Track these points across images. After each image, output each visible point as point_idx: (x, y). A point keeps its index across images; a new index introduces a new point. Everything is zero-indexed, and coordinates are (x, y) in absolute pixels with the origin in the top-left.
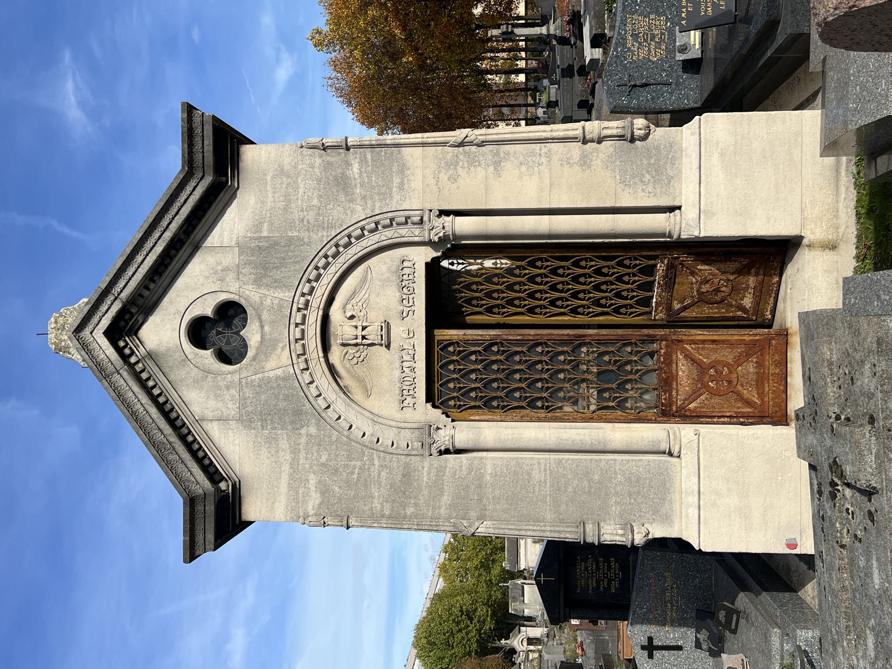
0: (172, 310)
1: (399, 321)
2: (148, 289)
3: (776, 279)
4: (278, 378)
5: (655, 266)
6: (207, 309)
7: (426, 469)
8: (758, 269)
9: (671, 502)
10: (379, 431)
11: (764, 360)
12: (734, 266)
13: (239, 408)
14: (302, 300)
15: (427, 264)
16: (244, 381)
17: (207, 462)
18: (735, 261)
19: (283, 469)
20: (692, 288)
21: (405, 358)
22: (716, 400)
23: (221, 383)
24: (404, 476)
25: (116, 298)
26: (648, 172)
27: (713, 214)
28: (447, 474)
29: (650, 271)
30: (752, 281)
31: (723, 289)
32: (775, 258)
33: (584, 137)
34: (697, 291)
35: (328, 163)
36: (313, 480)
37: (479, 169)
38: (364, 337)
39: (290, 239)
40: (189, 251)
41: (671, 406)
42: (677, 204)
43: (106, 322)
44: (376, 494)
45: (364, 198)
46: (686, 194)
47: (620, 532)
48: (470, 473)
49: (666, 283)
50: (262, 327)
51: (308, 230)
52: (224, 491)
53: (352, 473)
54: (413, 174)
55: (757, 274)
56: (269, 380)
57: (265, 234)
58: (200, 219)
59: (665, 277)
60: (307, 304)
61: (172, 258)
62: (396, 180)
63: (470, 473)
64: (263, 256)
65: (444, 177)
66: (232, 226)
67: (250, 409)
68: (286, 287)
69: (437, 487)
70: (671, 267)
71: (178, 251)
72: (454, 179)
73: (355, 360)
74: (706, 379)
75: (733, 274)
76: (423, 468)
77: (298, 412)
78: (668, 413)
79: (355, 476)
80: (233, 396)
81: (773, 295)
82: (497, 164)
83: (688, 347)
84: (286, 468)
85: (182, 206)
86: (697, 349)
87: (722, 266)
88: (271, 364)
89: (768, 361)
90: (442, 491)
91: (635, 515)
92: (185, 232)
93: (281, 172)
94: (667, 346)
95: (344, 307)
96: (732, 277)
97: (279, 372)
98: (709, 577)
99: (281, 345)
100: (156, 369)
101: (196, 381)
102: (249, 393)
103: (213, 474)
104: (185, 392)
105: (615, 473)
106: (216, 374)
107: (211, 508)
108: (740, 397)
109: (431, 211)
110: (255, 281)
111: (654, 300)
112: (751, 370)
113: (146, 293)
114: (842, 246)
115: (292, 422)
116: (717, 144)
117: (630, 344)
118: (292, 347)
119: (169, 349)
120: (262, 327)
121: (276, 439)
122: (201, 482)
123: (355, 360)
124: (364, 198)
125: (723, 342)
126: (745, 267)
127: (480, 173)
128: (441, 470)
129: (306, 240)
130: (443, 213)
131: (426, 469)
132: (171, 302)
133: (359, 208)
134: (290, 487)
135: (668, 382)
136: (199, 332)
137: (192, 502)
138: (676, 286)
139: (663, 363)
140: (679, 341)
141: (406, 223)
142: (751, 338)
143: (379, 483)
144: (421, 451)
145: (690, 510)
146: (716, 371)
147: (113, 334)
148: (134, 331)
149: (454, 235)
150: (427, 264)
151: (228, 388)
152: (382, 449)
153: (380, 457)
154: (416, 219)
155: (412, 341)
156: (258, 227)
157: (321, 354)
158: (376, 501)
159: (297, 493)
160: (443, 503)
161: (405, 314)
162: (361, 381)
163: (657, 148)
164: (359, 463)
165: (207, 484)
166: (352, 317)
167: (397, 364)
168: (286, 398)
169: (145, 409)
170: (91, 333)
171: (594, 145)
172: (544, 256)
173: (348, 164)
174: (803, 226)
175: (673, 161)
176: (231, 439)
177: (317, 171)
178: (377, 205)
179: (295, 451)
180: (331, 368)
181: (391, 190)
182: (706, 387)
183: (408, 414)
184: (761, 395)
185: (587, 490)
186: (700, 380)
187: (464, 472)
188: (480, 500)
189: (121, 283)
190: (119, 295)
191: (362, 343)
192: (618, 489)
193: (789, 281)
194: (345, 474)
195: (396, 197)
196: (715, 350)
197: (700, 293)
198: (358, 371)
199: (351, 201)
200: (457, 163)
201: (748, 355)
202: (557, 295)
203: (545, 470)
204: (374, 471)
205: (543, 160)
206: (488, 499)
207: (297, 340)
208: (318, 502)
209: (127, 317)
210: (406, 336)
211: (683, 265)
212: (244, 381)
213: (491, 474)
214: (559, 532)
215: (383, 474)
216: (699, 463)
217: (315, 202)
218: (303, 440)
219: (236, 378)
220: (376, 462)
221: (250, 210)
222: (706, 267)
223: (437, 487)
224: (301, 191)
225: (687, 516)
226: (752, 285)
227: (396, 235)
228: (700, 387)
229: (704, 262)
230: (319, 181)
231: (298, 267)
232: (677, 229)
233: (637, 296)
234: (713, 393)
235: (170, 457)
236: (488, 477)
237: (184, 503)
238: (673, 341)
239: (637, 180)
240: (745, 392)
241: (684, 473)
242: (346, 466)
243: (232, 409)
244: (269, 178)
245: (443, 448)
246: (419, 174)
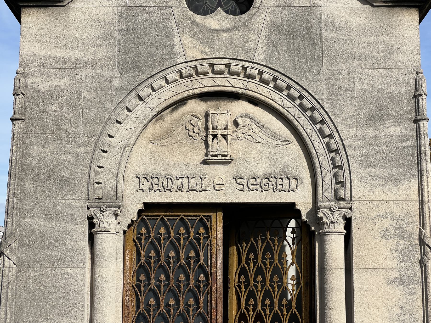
1: (232, 174)
4: (172, 46)
7: (74, 203)
19: (76, 51)
21: (192, 181)
24: (67, 179)
28: (68, 225)
35: (400, 101)
36: (63, 83)
37: (396, 261)
38: (215, 136)
39: (319, 60)
44: (47, 150)
48: (69, 250)
50: (226, 30)
51: (329, 79)
53: (71, 125)
54: (389, 190)
56: (170, 38)
57: (325, 34)
60: (251, 77)
62: (382, 172)
67: (140, 17)
68: (269, 56)
69: (55, 215)
72: (385, 234)
76: (75, 200)
77: (135, 67)
79: (67, 127)
82: (401, 281)
84: (77, 55)
90: (49, 219)
93: (390, 52)
95: (247, 116)
97: (178, 48)
99: (207, 50)
102: (156, 16)
109: (350, 209)
118: (205, 62)
120: (226, 30)
121: (107, 44)
124: (364, 138)
127: (392, 262)
128: (72, 219)
129: (318, 77)
131: (74, 203)
133: (353, 133)
134: (56, 59)
143: (59, 153)
144: (92, 197)
149: (325, 234)
150: (294, 204)
152: (95, 156)
154: (341, 194)
156: (333, 26)
157: (197, 91)
158: (40, 149)
159: (50, 67)
160: (36, 220)
161: (239, 180)
162: (168, 133)
164: (80, 131)
166: (236, 124)
167: (185, 172)
168: (151, 55)
173: (400, 121)
177: (392, 89)
178: (356, 152)
179: (94, 64)
180: (182, 102)
181: (373, 166)
183: (132, 184)
187: (70, 244)
188: (39, 261)
191: (209, 135)
194: (69, 117)
195: (365, 172)
199: (360, 125)
200: (401, 238)
204: (73, 148)
207: (212, 66)
208: (40, 87)
210: (216, 182)
212: (170, 11)
215: (69, 156)
217: (359, 87)
218: (106, 73)
220: (82, 150)
221: (349, 19)
224: (370, 72)
230: (381, 91)
231: (290, 68)
242: (78, 118)
244: (384, 38)
245: (95, 221)
246: (391, 196)
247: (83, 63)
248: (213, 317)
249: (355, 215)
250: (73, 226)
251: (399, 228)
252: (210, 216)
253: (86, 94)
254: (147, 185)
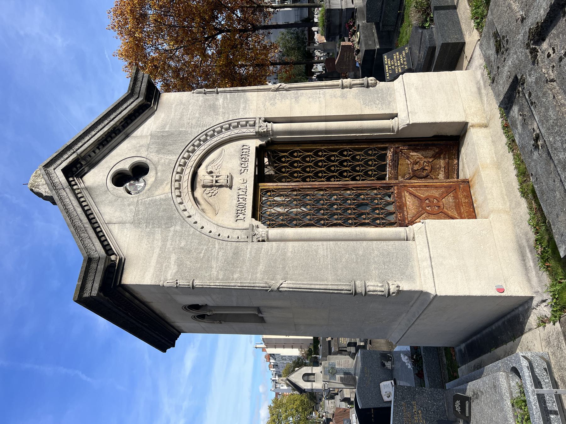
0: (106, 166)
2: (95, 153)
3: (456, 162)
4: (161, 199)
5: (386, 154)
6: (126, 166)
7: (249, 250)
8: (445, 155)
9: (412, 267)
10: (220, 230)
11: (457, 195)
12: (431, 153)
13: (134, 216)
14: (183, 160)
16: (140, 201)
17: (106, 243)
18: (431, 149)
19: (155, 251)
20: (408, 168)
21: (240, 194)
23: (125, 203)
24: (234, 254)
25: (74, 152)
26: (377, 99)
27: (416, 113)
28: (263, 252)
29: (383, 157)
30: (442, 162)
31: (426, 168)
32: (453, 148)
33: (343, 84)
34: (412, 169)
35: (206, 99)
36: (173, 257)
37: (287, 100)
38: (216, 182)
39: (180, 132)
40: (123, 137)
41: (404, 221)
42: (395, 112)
43: (64, 164)
44: (215, 266)
45: (224, 113)
46: (399, 107)
47: (380, 285)
48: (277, 251)
49: (393, 164)
50: (157, 173)
51: (191, 128)
52: (113, 261)
53: (200, 253)
54: (251, 103)
55: (444, 158)
56: (156, 201)
57: (167, 130)
58: (132, 121)
59: (392, 160)
60: (185, 164)
61: (112, 138)
62: (242, 106)
63: (277, 251)
64: (163, 140)
65: (268, 104)
66: (150, 126)
67: (140, 217)
68: (175, 154)
69: (256, 260)
70: (395, 153)
71: (116, 135)
72: (273, 105)
73: (210, 194)
74: (424, 205)
75: (431, 158)
76: (247, 249)
77: (170, 218)
78: (403, 224)
79: (202, 255)
80: (131, 210)
81: (456, 172)
82: (297, 98)
83: (410, 189)
84: (157, 250)
85: (123, 110)
86: (417, 190)
87: (424, 153)
88: (159, 191)
89: (460, 195)
90: (258, 263)
91: (389, 276)
92: (122, 126)
94: (398, 189)
95: (207, 167)
96: (431, 160)
97: (163, 196)
98: (443, 405)
99: (166, 182)
100: (88, 195)
101: (110, 202)
102: (141, 208)
103: (108, 250)
104: (102, 208)
105: (373, 250)
106: (123, 198)
107: (101, 267)
109: (260, 118)
110: (157, 151)
111: (387, 176)
112: (451, 200)
113: (93, 154)
114: (492, 125)
115: (166, 224)
116: (413, 84)
117: (376, 189)
118: (173, 183)
119: (99, 185)
120: (157, 173)
121: (154, 234)
122: (98, 250)
123: (210, 194)
125: (431, 186)
126: (437, 153)
127: (288, 102)
128: (259, 250)
129: (189, 132)
130: (266, 120)
131: (249, 250)
132: (106, 162)
133: (221, 118)
134: (158, 262)
135: (401, 207)
136: (120, 179)
137: (89, 260)
138: (399, 166)
139: (396, 197)
140: (405, 186)
141: (246, 126)
142: (448, 184)
143: (217, 259)
144: (247, 240)
145: (426, 271)
146: (429, 201)
147: (68, 172)
148: (81, 176)
149: (272, 130)
150: (256, 148)
151: (129, 205)
152: (221, 239)
153: (219, 243)
154: (252, 123)
155: (245, 185)
156: (164, 126)
157: (190, 190)
158: (214, 270)
159: (162, 265)
160: (259, 270)
161: (242, 171)
163: (382, 90)
164: (205, 247)
165: (102, 252)
166: (211, 172)
167: (236, 197)
169: (74, 208)
170: (54, 169)
171: (348, 89)
172: (323, 148)
173: (217, 99)
174: (466, 117)
175: (390, 95)
176: (125, 234)
179: (164, 240)
180: (195, 199)
181: (239, 109)
182: (424, 209)
183: (241, 224)
185: (355, 261)
186: (421, 206)
187: (274, 251)
188: (284, 268)
189: (80, 144)
190: (76, 150)
191: (216, 185)
192: (376, 259)
193: (464, 156)
194: (195, 254)
196: (427, 191)
197: (414, 171)
198: (211, 201)
199: (217, 115)
200: (275, 98)
201: (448, 193)
202: (331, 174)
203: (327, 249)
204: (215, 252)
205: (321, 96)
206: (289, 267)
207: (176, 181)
208: (174, 271)
209: (79, 166)
210: (242, 182)
211: (402, 152)
212: (140, 201)
213: (292, 252)
214: (337, 285)
215: (220, 253)
216: (428, 243)
217: (197, 115)
219: (135, 200)
220: (217, 246)
221: (161, 119)
222: (415, 154)
223: (256, 260)
225: (424, 275)
226: (443, 166)
227: (240, 132)
229: (415, 150)
230: (200, 107)
231: (183, 144)
232: (397, 124)
233: (377, 174)
235: (82, 235)
236: (289, 254)
237: (84, 260)
238: (401, 186)
239: (372, 103)
240: (449, 212)
241: (418, 249)
242: (197, 249)
243: (129, 216)
244: (174, 106)
245: (260, 239)
247: (163, 248)
248: (316, 186)
249: (263, 116)
250: (263, 250)
251: (270, 99)
252: (261, 189)
253: (183, 244)
254: (241, 216)
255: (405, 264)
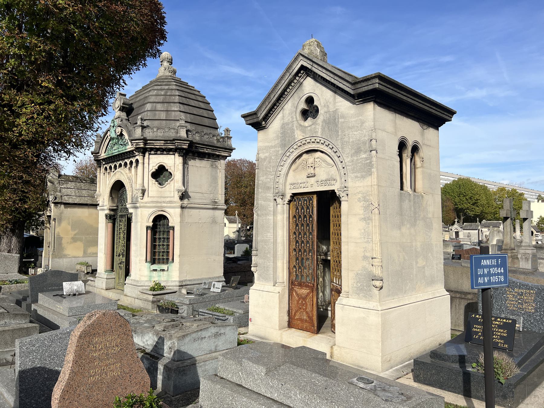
1: (315, 180)
15: (334, 190)
22: (296, 302)
26: (361, 285)
27: (342, 310)
36: (267, 155)
37: (363, 211)
43: (305, 64)
56: (294, 133)
62: (359, 175)
66: (343, 105)
68: (322, 134)
69: (266, 199)
72: (359, 200)
84: (270, 144)
90: (264, 201)
93: (363, 123)
97: (296, 136)
103: (266, 117)
107: (255, 120)
108: (296, 312)
120: (309, 126)
122: (261, 115)
124: (353, 161)
127: (361, 212)
128: (270, 200)
133: (349, 160)
143: (266, 179)
156: (343, 117)
162: (297, 168)
165: (261, 118)
167: (302, 181)
168: (289, 140)
173: (365, 152)
174: (339, 347)
177: (363, 139)
178: (350, 167)
180: (300, 156)
181: (355, 173)
184: (297, 319)
188: (263, 215)
195: (353, 175)
201: (309, 317)
205: (366, 240)
217: (351, 140)
218: (277, 149)
223: (266, 199)
224: (355, 133)
228: (300, 297)
230: (359, 140)
234: (298, 301)
243: (286, 120)
246: (361, 184)
247: (272, 147)
251: (364, 197)
253: (273, 158)
255: (265, 278)
